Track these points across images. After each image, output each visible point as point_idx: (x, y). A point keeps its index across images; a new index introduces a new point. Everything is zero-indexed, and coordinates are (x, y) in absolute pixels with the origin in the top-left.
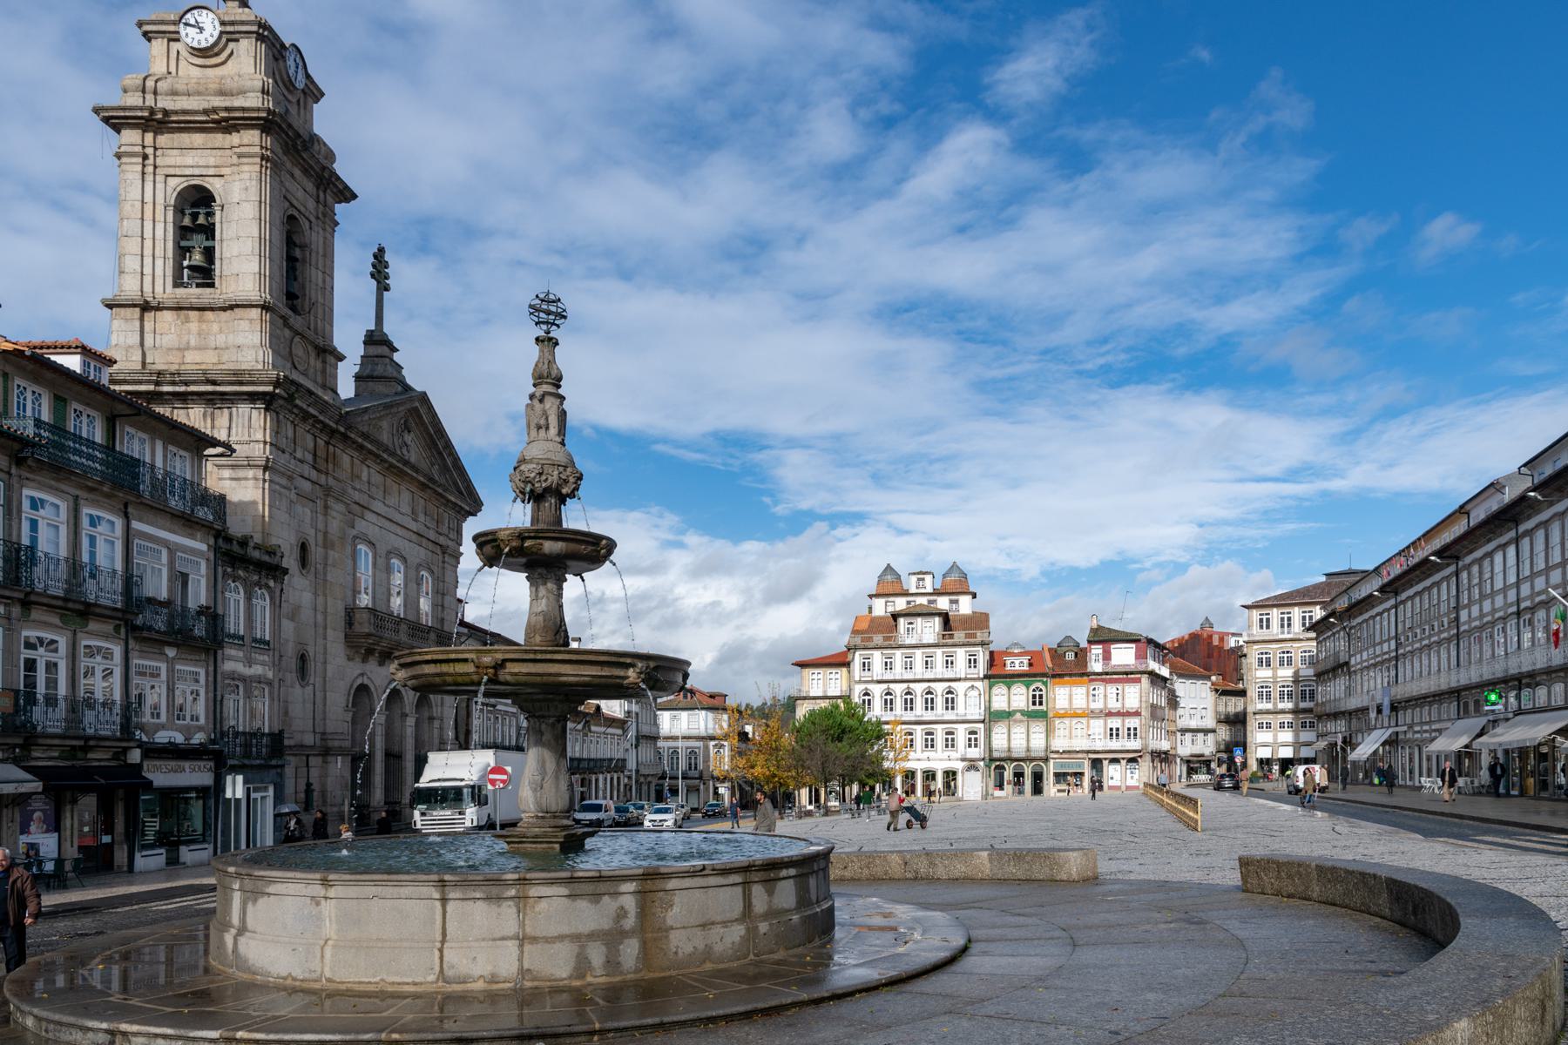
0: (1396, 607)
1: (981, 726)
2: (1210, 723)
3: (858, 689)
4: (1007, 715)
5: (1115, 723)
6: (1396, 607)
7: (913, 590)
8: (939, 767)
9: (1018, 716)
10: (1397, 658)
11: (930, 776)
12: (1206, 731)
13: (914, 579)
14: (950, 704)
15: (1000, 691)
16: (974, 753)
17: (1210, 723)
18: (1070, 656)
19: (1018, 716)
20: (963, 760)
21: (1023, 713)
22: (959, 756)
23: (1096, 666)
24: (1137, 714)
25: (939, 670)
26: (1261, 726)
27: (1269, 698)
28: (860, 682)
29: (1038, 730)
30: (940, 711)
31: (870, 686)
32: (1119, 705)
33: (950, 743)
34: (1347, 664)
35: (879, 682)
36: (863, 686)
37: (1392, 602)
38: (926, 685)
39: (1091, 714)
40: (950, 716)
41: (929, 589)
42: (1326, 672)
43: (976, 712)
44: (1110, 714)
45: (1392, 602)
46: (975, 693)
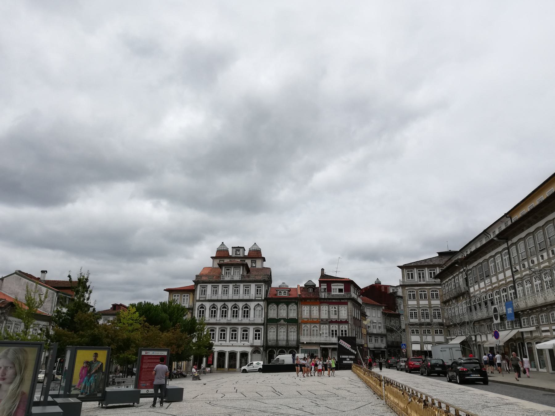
0: (508, 248)
1: (262, 327)
2: (383, 331)
3: (198, 304)
4: (275, 321)
5: (334, 327)
6: (508, 248)
7: (234, 255)
8: (239, 350)
9: (282, 321)
10: (514, 282)
11: (233, 355)
12: (382, 335)
13: (234, 250)
14: (246, 314)
15: (273, 307)
16: (258, 343)
17: (383, 331)
18: (311, 290)
19: (282, 321)
20: (251, 346)
21: (284, 320)
22: (249, 344)
23: (323, 295)
24: (346, 322)
25: (241, 296)
26: (413, 332)
27: (416, 317)
28: (199, 301)
29: (293, 329)
30: (240, 318)
31: (204, 303)
32: (336, 317)
33: (245, 337)
34: (468, 292)
35: (209, 301)
36: (200, 303)
37: (505, 246)
38: (233, 303)
39: (322, 322)
40: (246, 321)
41: (241, 255)
42: (448, 301)
43: (260, 320)
44: (331, 322)
45: (505, 246)
46: (259, 308)
